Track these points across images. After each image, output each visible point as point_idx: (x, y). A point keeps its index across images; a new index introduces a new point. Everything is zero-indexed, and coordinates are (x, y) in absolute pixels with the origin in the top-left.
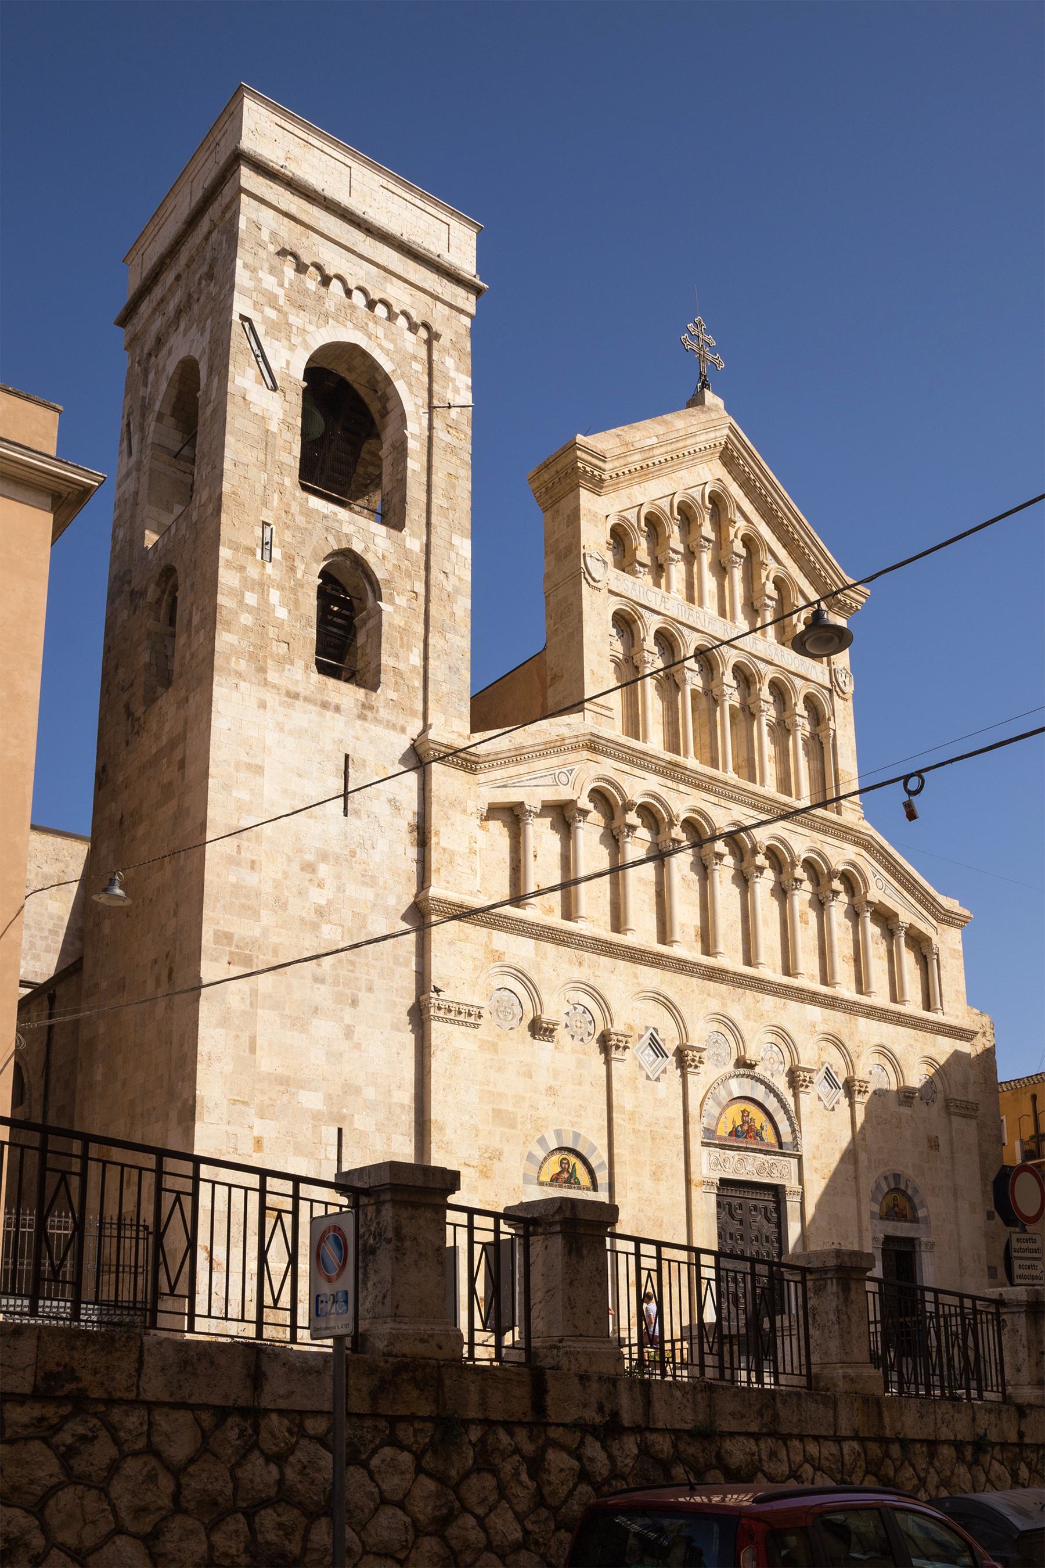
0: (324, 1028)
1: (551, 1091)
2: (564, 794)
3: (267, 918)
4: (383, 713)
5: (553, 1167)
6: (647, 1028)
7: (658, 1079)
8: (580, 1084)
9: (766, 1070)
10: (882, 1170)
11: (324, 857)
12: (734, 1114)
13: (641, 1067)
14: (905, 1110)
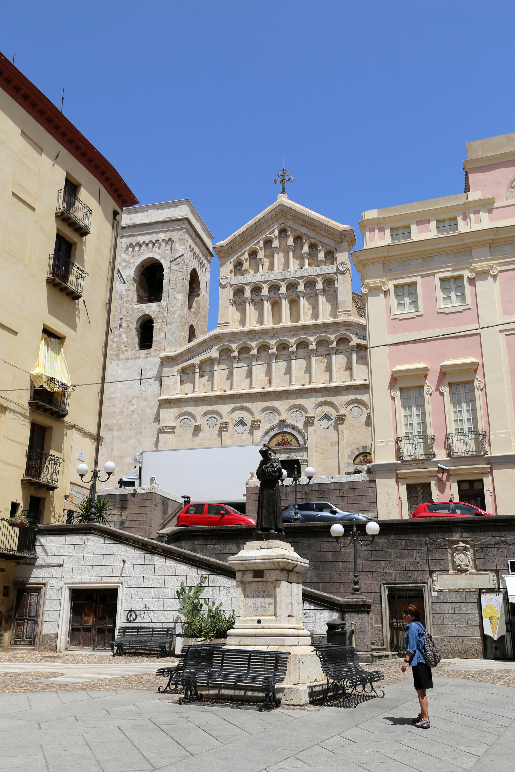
0: (132, 442)
3: (118, 418)
4: (152, 354)
6: (239, 418)
7: (243, 433)
8: (211, 440)
9: (293, 421)
10: (355, 446)
11: (134, 398)
12: (279, 438)
13: (236, 431)
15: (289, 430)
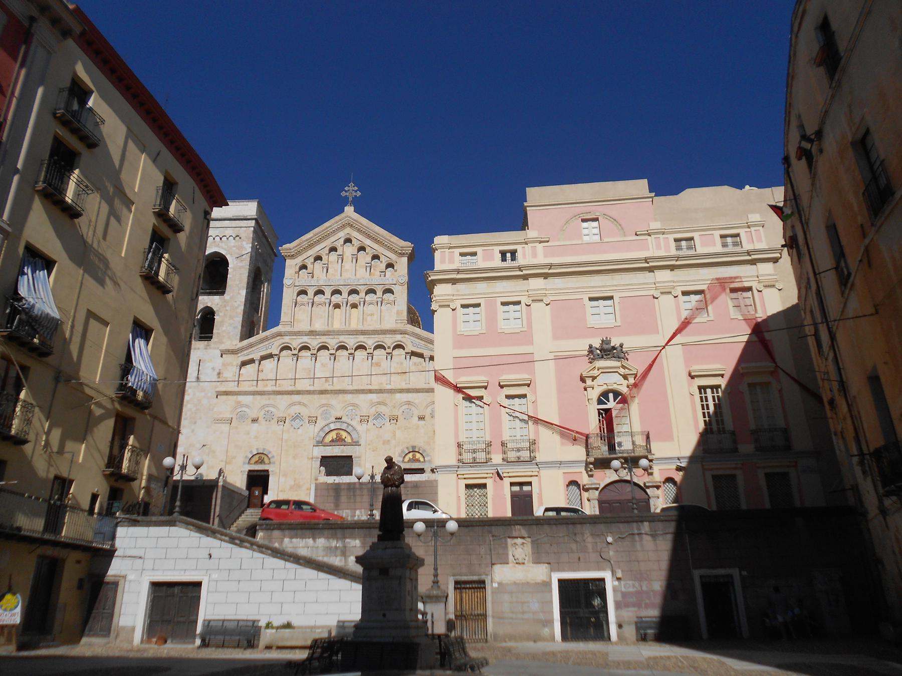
1: (256, 437)
2: (269, 352)
5: (256, 458)
12: (333, 435)
14: (422, 422)
15: (344, 426)
